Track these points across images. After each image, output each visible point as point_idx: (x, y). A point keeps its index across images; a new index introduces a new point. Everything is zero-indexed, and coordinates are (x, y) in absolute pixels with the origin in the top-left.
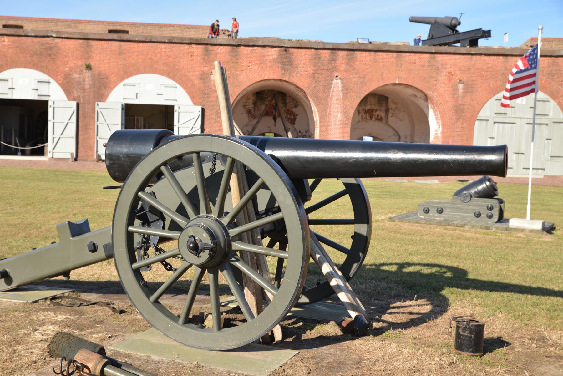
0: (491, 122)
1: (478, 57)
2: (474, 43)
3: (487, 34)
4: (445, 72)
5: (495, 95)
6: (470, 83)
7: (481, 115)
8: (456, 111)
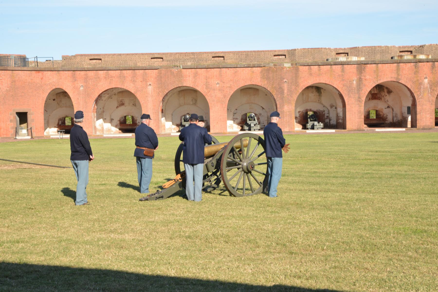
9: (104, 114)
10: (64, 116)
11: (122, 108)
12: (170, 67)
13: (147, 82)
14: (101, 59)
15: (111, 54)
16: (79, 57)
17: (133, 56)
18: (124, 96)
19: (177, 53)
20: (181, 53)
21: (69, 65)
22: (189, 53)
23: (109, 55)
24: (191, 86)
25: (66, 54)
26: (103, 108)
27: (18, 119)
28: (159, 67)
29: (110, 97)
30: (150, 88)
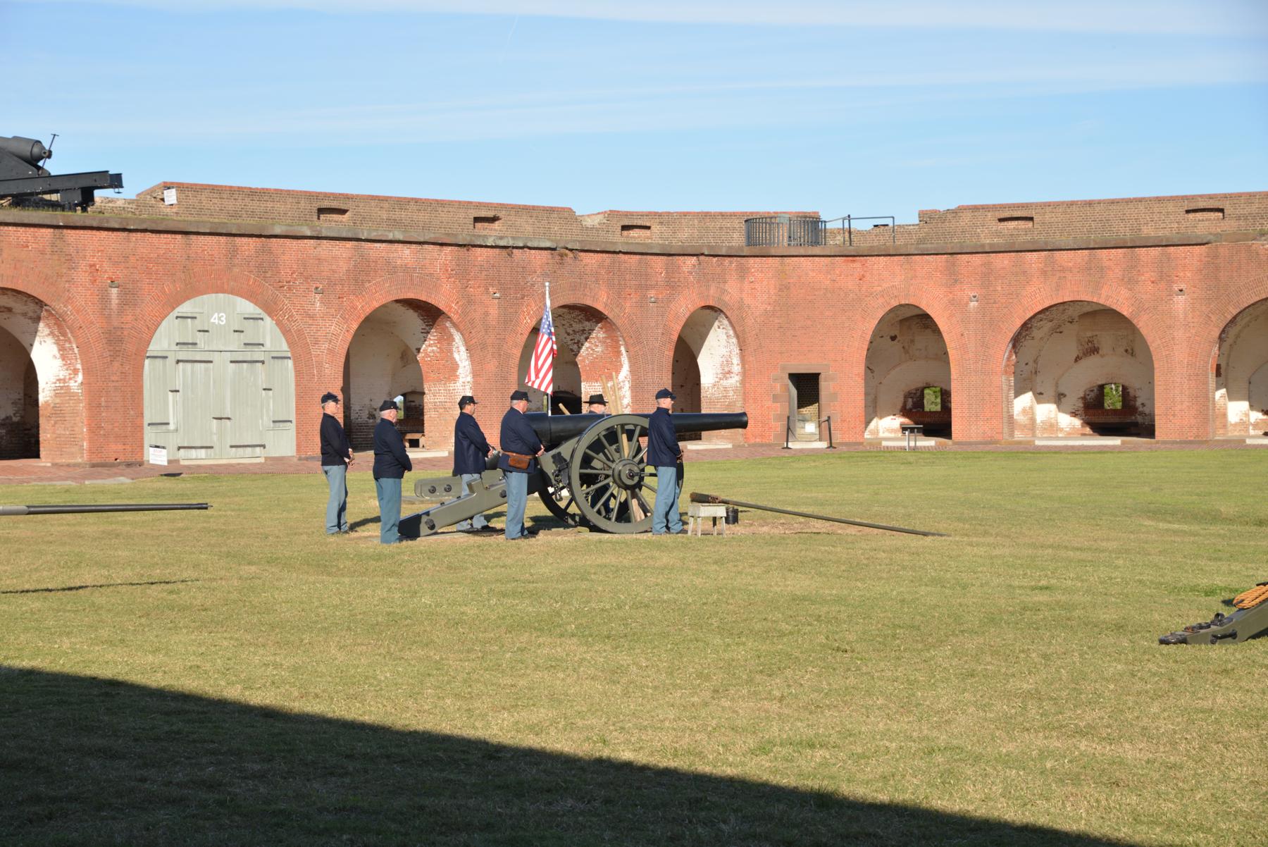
0: (171, 361)
1: (139, 234)
2: (87, 198)
3: (115, 181)
4: (83, 265)
5: (174, 309)
6: (130, 286)
7: (154, 348)
8: (109, 342)
9: (1039, 379)
10: (920, 385)
11: (1093, 360)
12: (1246, 237)
13: (1170, 282)
14: (1031, 219)
15: (1063, 203)
16: (969, 214)
17: (1131, 205)
18: (1098, 326)
21: (940, 239)
23: (1057, 205)
25: (928, 206)
26: (1035, 361)
27: (794, 392)
28: (1211, 237)
29: (1057, 330)
30: (1180, 302)
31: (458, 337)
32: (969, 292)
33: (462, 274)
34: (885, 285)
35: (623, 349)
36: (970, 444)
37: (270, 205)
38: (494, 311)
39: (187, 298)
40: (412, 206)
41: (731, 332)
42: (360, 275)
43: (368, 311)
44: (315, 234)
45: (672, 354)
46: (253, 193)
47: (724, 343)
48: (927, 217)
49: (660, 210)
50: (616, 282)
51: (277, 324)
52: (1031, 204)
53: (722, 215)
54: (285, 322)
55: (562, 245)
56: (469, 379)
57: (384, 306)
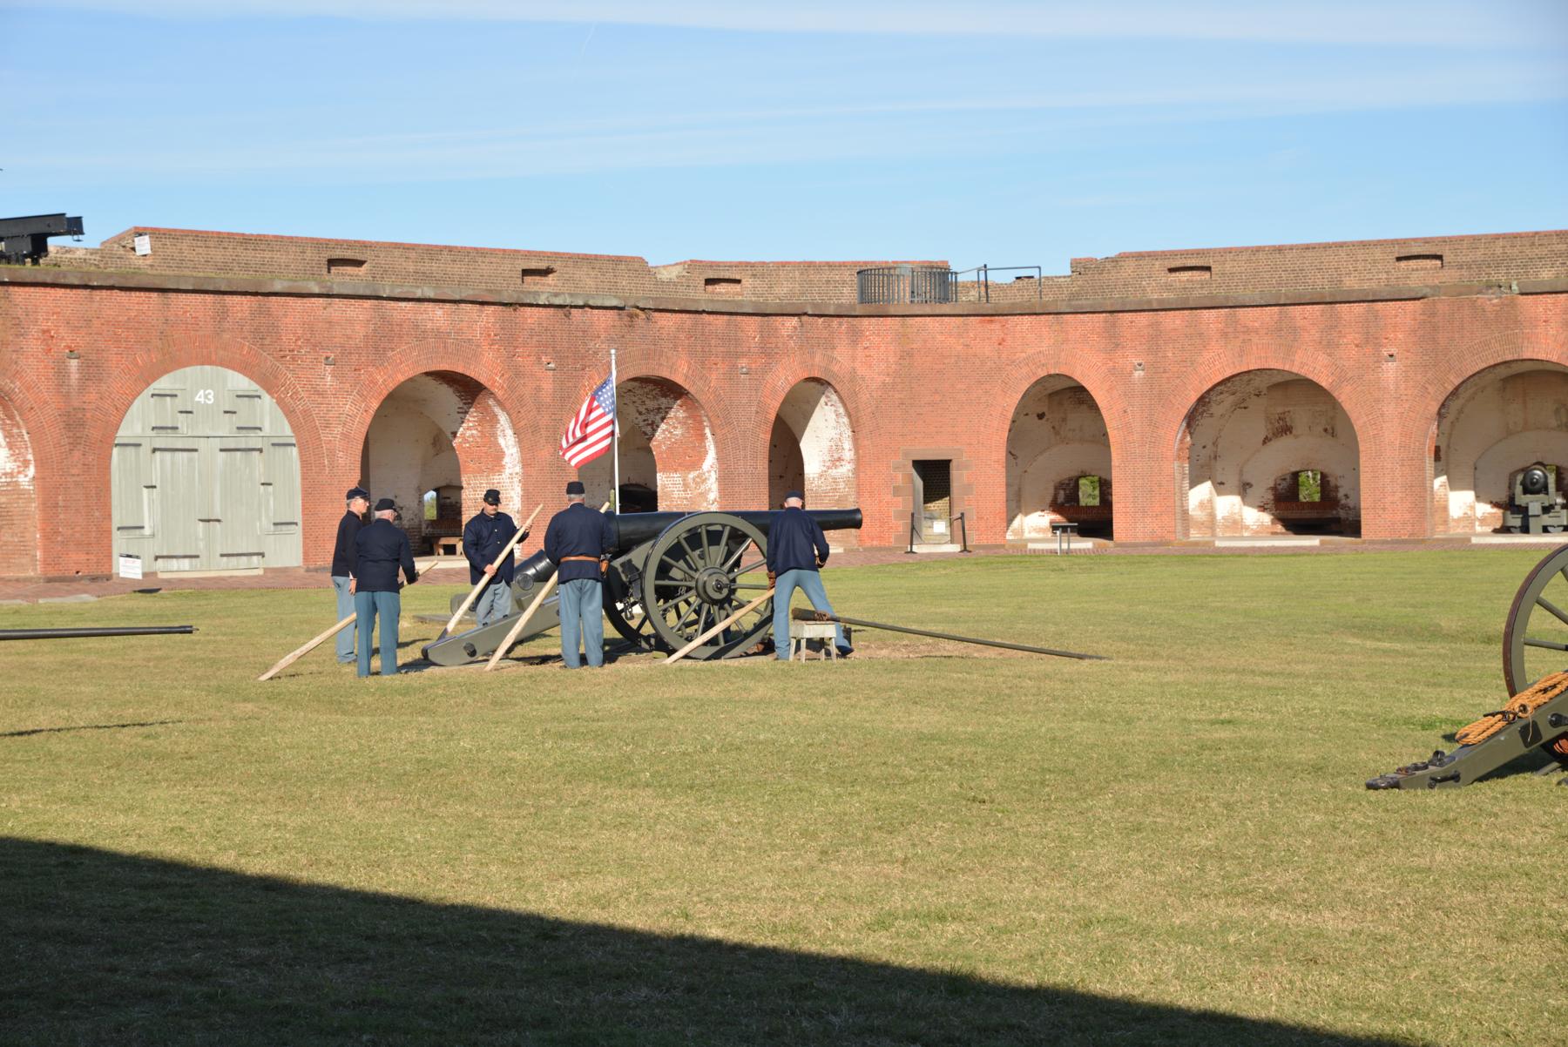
0: (145, 449)
1: (104, 293)
2: (39, 248)
3: (74, 226)
4: (34, 331)
6: (94, 357)
7: (125, 433)
8: (68, 426)
10: (1074, 474)
11: (1285, 441)
12: (1469, 290)
14: (1208, 269)
15: (1247, 249)
16: (1132, 263)
18: (1290, 400)
19: (1497, 237)
20: (1516, 236)
21: (1097, 293)
22: (1548, 235)
23: (1240, 251)
24: (1555, 359)
27: (919, 483)
29: (1241, 405)
30: (1391, 365)
31: (503, 418)
32: (1133, 359)
33: (508, 340)
34: (1030, 351)
35: (707, 431)
36: (1135, 545)
37: (268, 255)
38: (548, 386)
39: (166, 371)
40: (445, 255)
41: (841, 410)
42: (381, 343)
43: (392, 386)
44: (324, 291)
45: (768, 437)
46: (246, 240)
47: (832, 423)
48: (1081, 267)
49: (753, 260)
50: (699, 349)
51: (278, 403)
52: (1209, 251)
53: (830, 265)
54: (288, 400)
55: (632, 303)
56: (518, 469)
57: (411, 380)
